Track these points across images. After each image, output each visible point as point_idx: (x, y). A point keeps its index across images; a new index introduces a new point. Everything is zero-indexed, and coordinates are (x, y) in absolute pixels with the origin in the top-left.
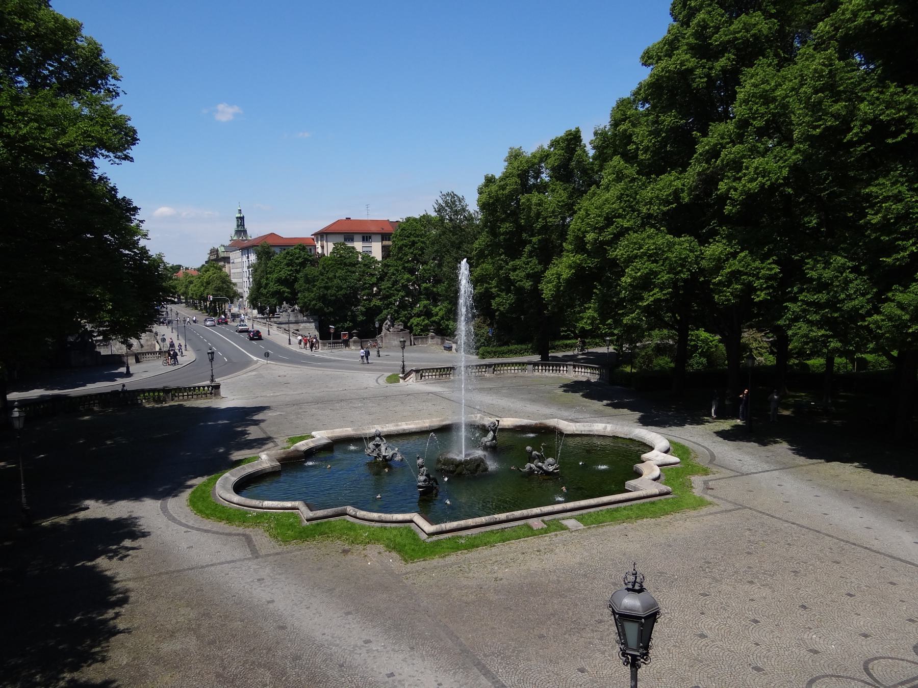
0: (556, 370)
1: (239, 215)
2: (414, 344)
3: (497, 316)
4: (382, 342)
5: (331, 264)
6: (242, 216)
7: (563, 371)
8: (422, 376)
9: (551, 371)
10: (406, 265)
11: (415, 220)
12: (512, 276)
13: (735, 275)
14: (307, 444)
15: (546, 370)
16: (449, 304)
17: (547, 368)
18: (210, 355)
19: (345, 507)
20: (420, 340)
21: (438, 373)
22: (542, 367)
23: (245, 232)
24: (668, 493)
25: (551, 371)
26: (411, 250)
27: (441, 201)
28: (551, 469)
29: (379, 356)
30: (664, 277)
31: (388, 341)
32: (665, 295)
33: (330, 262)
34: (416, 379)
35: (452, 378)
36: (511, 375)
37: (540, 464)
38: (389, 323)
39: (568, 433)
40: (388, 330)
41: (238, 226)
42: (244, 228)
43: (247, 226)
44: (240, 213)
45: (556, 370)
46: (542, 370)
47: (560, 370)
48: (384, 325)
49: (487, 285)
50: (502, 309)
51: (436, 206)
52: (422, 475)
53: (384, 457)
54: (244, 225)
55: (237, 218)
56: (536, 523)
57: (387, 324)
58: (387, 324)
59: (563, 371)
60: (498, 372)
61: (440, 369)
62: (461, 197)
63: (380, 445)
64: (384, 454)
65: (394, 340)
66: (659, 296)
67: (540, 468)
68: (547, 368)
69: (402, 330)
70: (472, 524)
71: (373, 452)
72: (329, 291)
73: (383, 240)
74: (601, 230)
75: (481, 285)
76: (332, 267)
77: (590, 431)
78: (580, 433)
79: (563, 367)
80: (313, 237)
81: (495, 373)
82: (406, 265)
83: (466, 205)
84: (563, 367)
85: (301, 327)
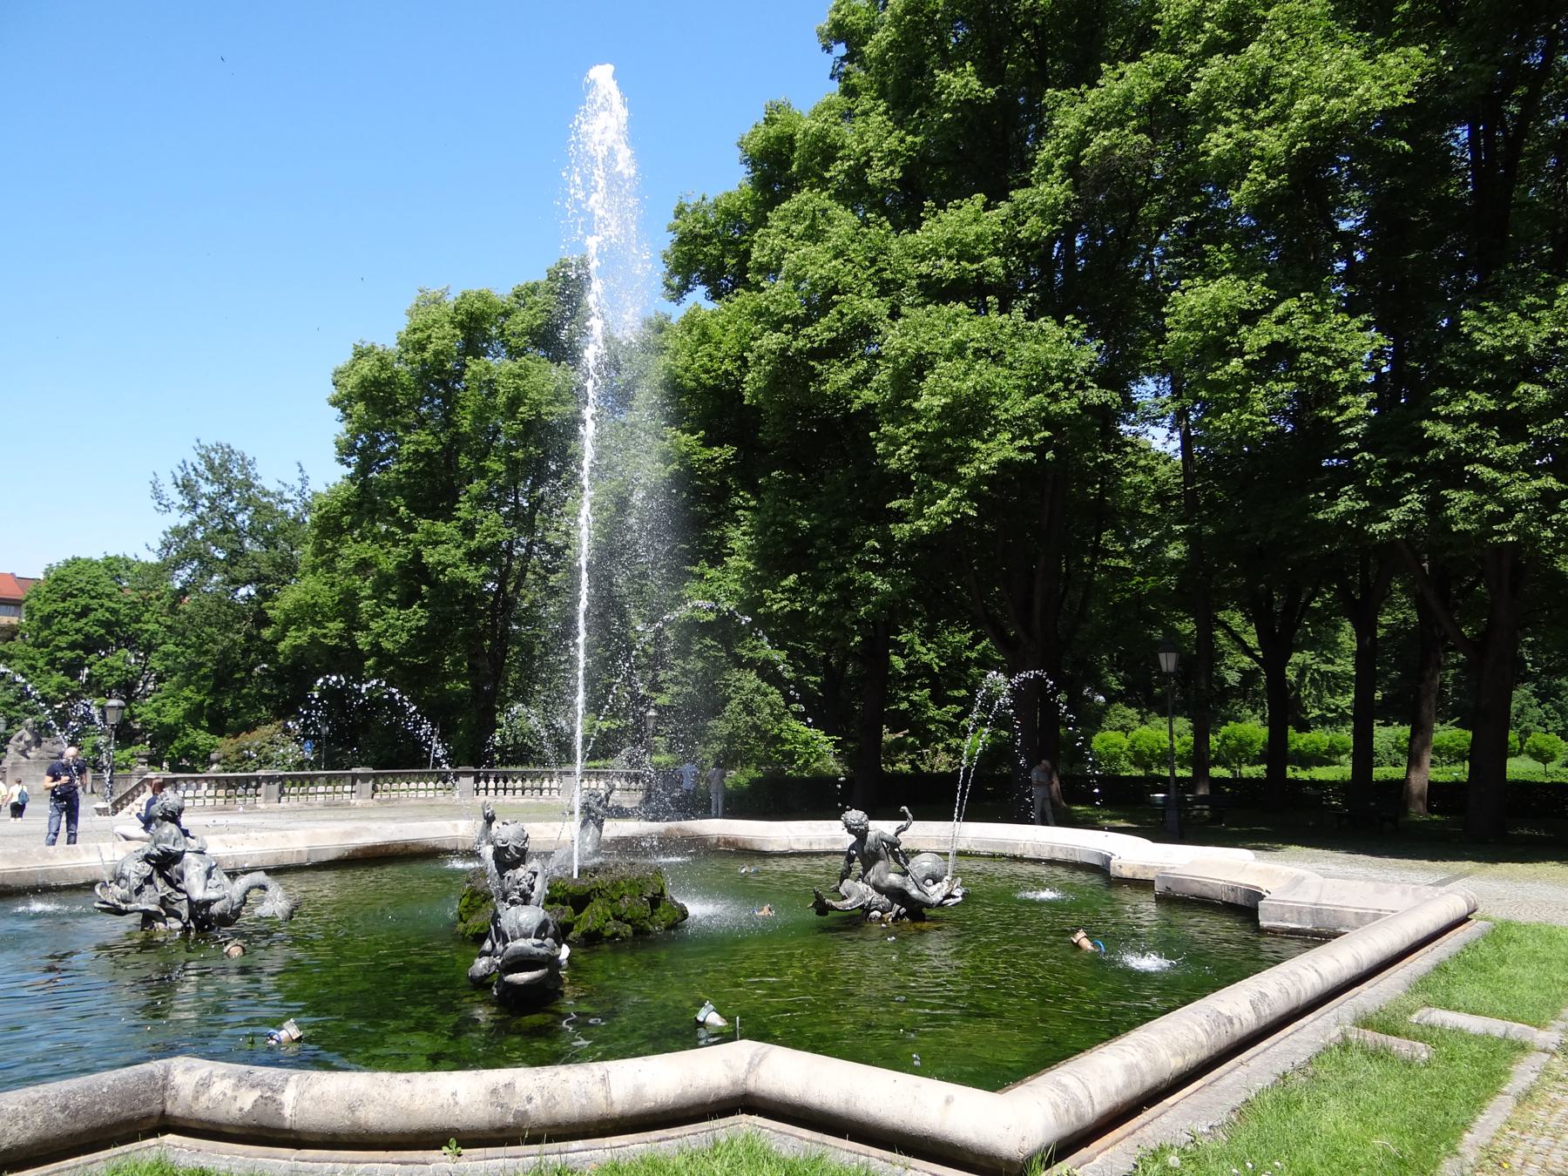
0: (532, 789)
2: (93, 792)
3: (370, 667)
9: (519, 792)
10: (59, 654)
11: (91, 563)
12: (430, 557)
13: (1280, 355)
15: (505, 790)
16: (199, 692)
19: (156, 1067)
22: (496, 781)
26: (77, 625)
27: (193, 458)
28: (935, 893)
30: (1019, 406)
32: (1022, 449)
35: (262, 806)
36: (420, 802)
37: (894, 879)
38: (28, 737)
40: (23, 753)
46: (496, 790)
49: (315, 630)
50: (387, 644)
51: (179, 475)
52: (526, 899)
53: (199, 909)
57: (21, 738)
58: (21, 738)
59: (550, 789)
60: (385, 796)
62: (249, 458)
63: (177, 857)
64: (198, 894)
66: (1009, 452)
67: (898, 895)
68: (510, 784)
71: (139, 891)
74: (799, 323)
75: (298, 630)
81: (377, 796)
82: (59, 654)
83: (257, 477)
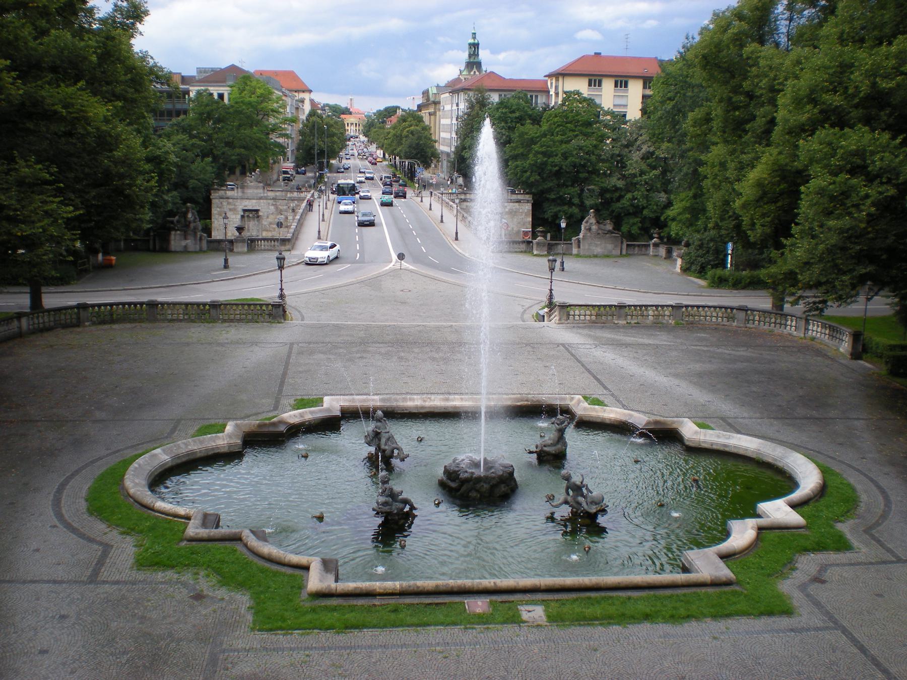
0: (781, 324)
1: (472, 41)
4: (579, 247)
6: (476, 41)
7: (791, 326)
9: (773, 325)
14: (301, 415)
17: (768, 320)
20: (636, 248)
23: (479, 65)
24: (728, 583)
25: (773, 325)
29: (563, 270)
33: (556, 119)
34: (560, 319)
39: (691, 444)
41: (470, 56)
43: (484, 55)
44: (474, 38)
45: (781, 324)
46: (759, 321)
47: (786, 325)
54: (478, 55)
55: (470, 44)
56: (479, 605)
59: (791, 326)
61: (598, 306)
65: (596, 246)
69: (610, 232)
70: (378, 590)
73: (645, 87)
76: (559, 126)
77: (725, 446)
79: (792, 321)
80: (547, 78)
84: (792, 321)
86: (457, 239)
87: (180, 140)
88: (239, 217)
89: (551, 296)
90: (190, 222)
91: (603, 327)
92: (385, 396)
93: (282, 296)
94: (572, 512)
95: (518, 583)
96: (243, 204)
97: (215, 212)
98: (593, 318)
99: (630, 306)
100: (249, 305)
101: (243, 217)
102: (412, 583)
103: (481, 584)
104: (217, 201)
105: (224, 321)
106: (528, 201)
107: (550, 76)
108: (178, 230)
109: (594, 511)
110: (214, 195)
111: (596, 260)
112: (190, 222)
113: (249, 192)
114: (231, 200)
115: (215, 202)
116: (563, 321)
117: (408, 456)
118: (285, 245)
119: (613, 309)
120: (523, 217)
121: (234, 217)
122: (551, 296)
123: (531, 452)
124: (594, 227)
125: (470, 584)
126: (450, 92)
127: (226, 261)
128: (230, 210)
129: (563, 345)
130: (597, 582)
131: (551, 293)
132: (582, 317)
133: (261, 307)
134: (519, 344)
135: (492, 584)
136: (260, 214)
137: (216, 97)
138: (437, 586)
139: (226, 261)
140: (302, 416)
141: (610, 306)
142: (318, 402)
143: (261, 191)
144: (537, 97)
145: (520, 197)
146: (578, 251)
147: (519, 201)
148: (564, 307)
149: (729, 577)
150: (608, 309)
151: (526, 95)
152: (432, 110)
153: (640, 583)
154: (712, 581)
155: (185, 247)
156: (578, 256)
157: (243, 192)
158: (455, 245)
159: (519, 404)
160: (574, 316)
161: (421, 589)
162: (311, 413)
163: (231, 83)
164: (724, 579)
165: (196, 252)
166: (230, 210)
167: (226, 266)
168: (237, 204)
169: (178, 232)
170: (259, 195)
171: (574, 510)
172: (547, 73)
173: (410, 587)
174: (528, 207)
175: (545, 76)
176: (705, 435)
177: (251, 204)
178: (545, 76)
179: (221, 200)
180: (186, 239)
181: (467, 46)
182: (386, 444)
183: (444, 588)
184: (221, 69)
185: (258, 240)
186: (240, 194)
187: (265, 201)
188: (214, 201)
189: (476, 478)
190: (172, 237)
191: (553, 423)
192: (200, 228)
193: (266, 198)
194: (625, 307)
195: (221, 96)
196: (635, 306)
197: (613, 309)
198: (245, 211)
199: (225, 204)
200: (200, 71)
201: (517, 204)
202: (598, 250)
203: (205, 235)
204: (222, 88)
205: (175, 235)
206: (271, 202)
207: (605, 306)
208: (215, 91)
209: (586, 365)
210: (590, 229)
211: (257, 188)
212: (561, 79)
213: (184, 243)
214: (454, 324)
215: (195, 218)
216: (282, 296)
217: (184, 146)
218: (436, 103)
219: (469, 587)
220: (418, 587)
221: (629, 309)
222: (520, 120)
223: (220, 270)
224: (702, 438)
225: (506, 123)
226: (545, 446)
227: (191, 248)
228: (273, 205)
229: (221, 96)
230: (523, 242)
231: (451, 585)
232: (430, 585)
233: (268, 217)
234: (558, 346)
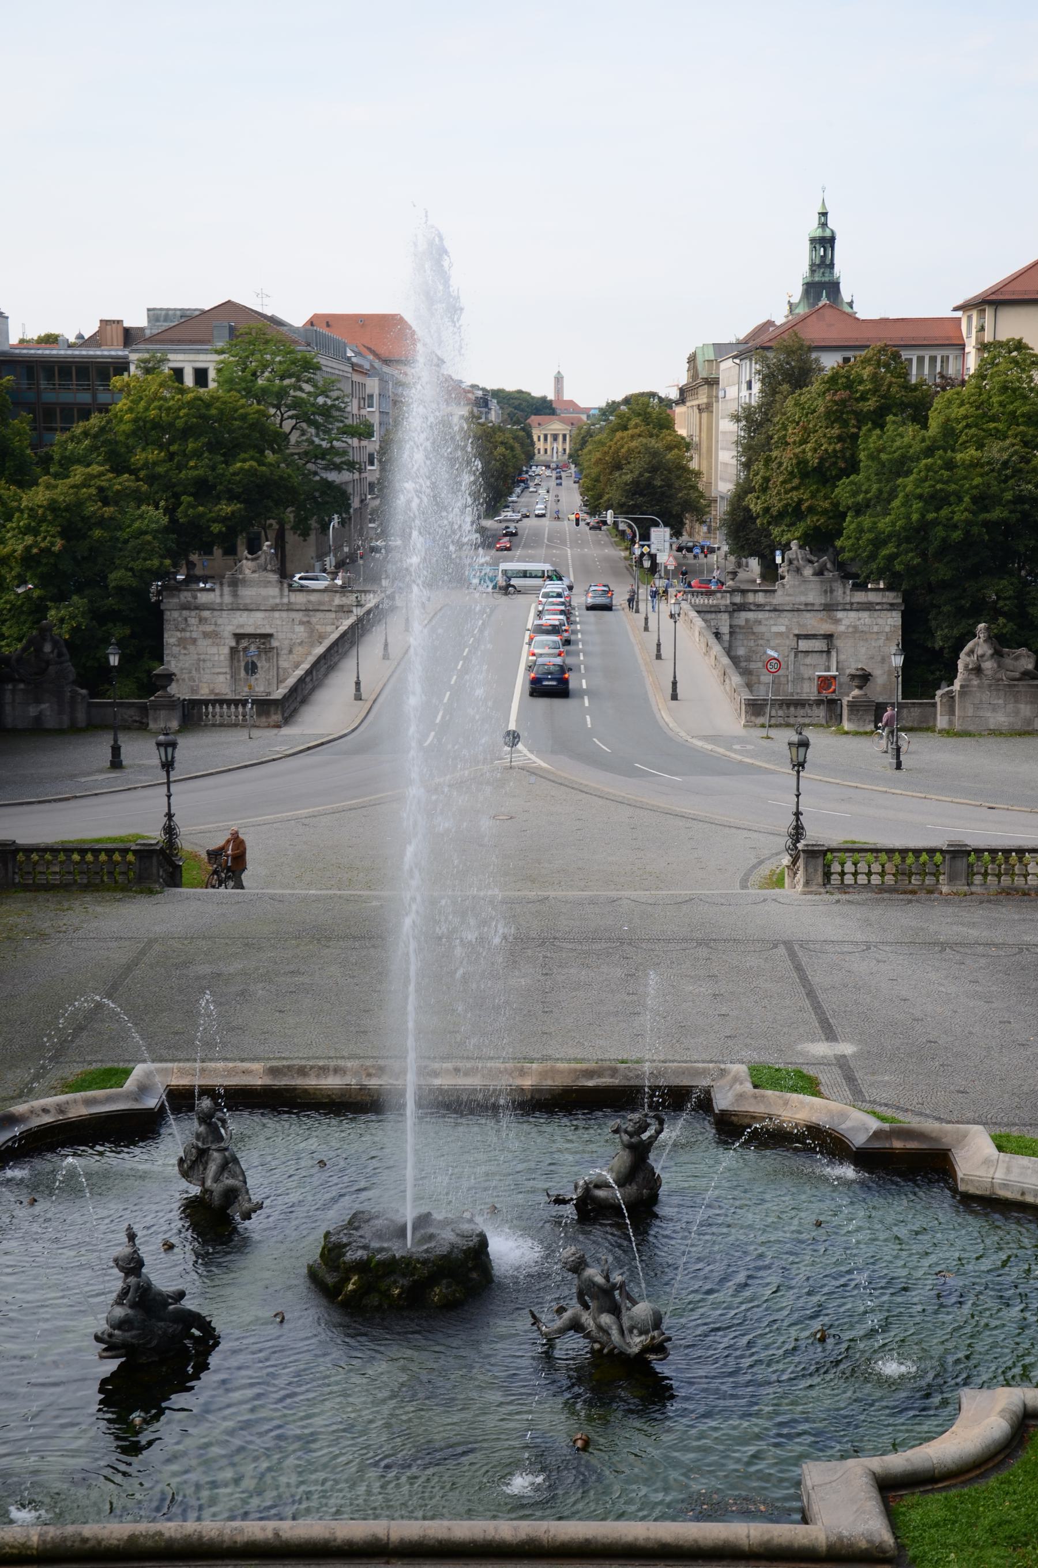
1: (819, 233)
4: (952, 712)
5: (966, 417)
6: (828, 234)
8: (827, 875)
14: (61, 1109)
18: (162, 750)
21: (890, 868)
23: (833, 288)
29: (899, 766)
31: (970, 712)
34: (807, 883)
39: (972, 1190)
41: (814, 268)
42: (832, 273)
43: (843, 268)
44: (824, 225)
48: (962, 655)
54: (832, 265)
55: (813, 241)
57: (972, 652)
65: (994, 709)
72: (944, 512)
76: (968, 426)
78: (1017, 1196)
80: (959, 314)
85: (842, 628)
86: (674, 697)
87: (93, 477)
88: (226, 651)
89: (798, 832)
90: (48, 663)
91: (910, 901)
92: (275, 1063)
93: (170, 830)
94: (592, 1351)
95: (277, 1535)
96: (235, 622)
97: (172, 641)
98: (889, 880)
99: (979, 852)
100: (83, 852)
101: (233, 651)
102: (70, 1529)
103: (241, 1531)
104: (175, 614)
105: (26, 888)
106: (892, 607)
107: (962, 308)
108: (22, 681)
109: (636, 1350)
110: (170, 603)
111: (991, 743)
112: (48, 663)
113: (248, 594)
114: (206, 614)
115: (172, 616)
116: (814, 888)
117: (260, 1206)
118: (267, 714)
119: (938, 857)
120: (881, 642)
121: (214, 650)
122: (798, 832)
123: (560, 1201)
124: (988, 665)
125: (214, 1534)
126: (735, 357)
127: (116, 750)
128: (206, 635)
129: (788, 945)
130: (533, 1534)
131: (798, 819)
132: (862, 879)
133: (110, 857)
134: (685, 940)
135: (270, 1534)
136: (275, 643)
137: (189, 380)
138: (132, 1538)
139: (116, 750)
140: (61, 1111)
141: (931, 852)
142: (116, 1076)
143: (274, 591)
144: (933, 360)
145: (872, 597)
146: (951, 722)
147: (868, 607)
148: (817, 855)
149: (877, 1540)
150: (924, 857)
151: (896, 356)
152: (703, 399)
153: (641, 1542)
154: (830, 1547)
155: (38, 719)
156: (948, 733)
157: (235, 594)
158: (665, 713)
159: (591, 1083)
160: (842, 874)
161: (92, 1543)
162: (88, 1102)
163: (220, 345)
164: (863, 1545)
165: (60, 732)
166: (206, 635)
167: (116, 764)
168: (220, 621)
169: (22, 686)
170: (272, 602)
171: (597, 1346)
172: (960, 302)
173: (64, 1539)
174: (894, 619)
175: (956, 309)
176: (1008, 1170)
177: (251, 622)
178: (956, 309)
179: (185, 613)
180: (38, 701)
181: (807, 245)
182: (216, 1180)
183: (150, 1543)
184: (204, 312)
185: (206, 702)
186: (228, 599)
187: (284, 614)
188: (167, 615)
189: (381, 1264)
190: (8, 697)
191: (616, 1131)
192: (72, 676)
193: (290, 608)
194: (968, 853)
195: (201, 375)
196: (993, 852)
197: (938, 857)
198: (239, 637)
199: (193, 621)
200: (154, 315)
201: (865, 615)
202: (999, 719)
203: (84, 692)
204: (202, 357)
205: (13, 691)
206: (298, 616)
207: (917, 852)
208: (187, 361)
209: (819, 992)
210: (978, 670)
211: (267, 584)
212: (989, 313)
213: (33, 711)
214: (552, 894)
215: (60, 655)
216: (170, 830)
217: (101, 489)
218: (712, 382)
219: (211, 1539)
220: (85, 1540)
221: (979, 859)
222: (878, 419)
223: (101, 771)
224: (1000, 1175)
225: (845, 424)
226: (598, 1186)
227: (50, 722)
228: (301, 623)
229: (201, 375)
230: (819, 703)
231: (167, 1535)
232: (116, 1535)
233: (290, 652)
234: (775, 946)
